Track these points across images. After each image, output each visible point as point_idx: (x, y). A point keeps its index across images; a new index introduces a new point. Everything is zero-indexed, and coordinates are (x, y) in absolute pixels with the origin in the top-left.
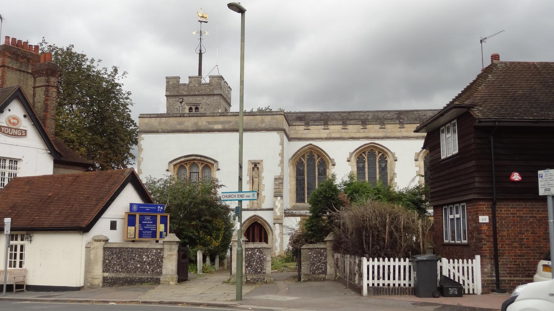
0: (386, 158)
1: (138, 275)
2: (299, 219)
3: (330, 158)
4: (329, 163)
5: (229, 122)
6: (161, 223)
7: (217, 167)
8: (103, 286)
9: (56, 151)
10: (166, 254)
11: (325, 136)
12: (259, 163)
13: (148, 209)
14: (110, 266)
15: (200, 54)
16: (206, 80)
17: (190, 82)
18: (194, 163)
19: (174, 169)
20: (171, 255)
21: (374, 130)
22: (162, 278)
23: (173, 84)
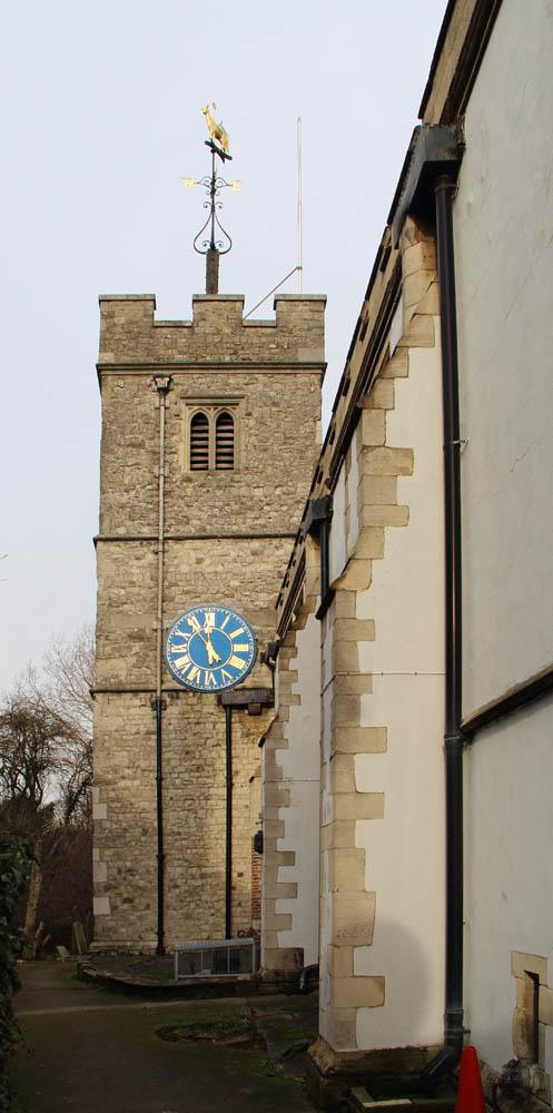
15: (213, 255)
23: (131, 322)
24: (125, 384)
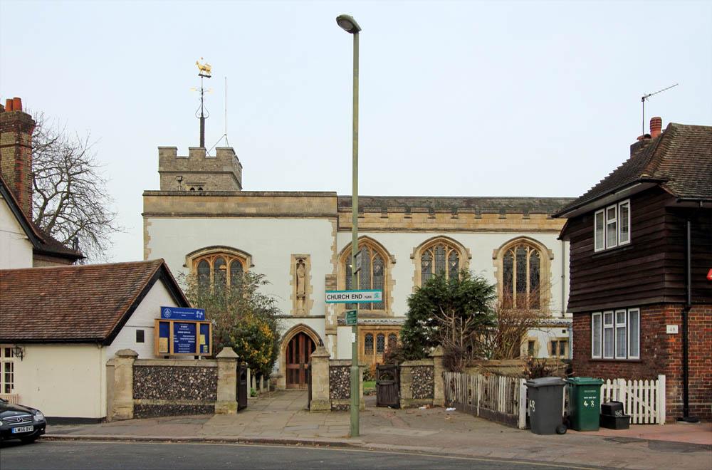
0: (457, 255)
1: (183, 402)
3: (389, 255)
4: (387, 259)
5: (266, 205)
6: (201, 333)
7: (251, 262)
8: (135, 417)
9: (36, 237)
10: (221, 374)
11: (382, 226)
12: (305, 259)
13: (184, 314)
14: (143, 391)
15: (202, 119)
16: (212, 153)
17: (191, 155)
18: (220, 257)
19: (193, 264)
20: (228, 376)
21: (444, 220)
22: (217, 407)
23: (168, 157)
24: (168, 178)
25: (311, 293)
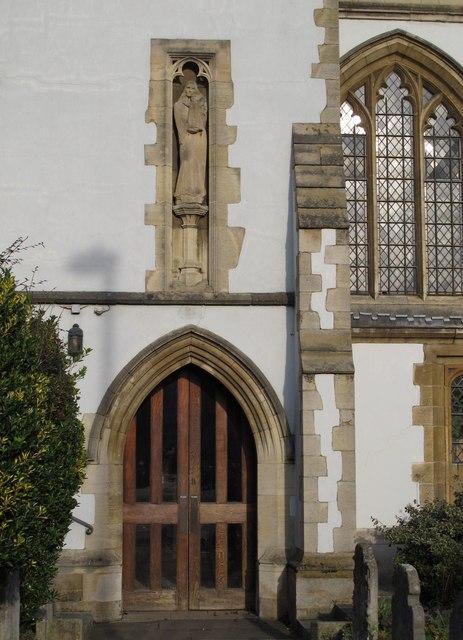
2: (413, 353)
12: (208, 57)
25: (237, 200)
